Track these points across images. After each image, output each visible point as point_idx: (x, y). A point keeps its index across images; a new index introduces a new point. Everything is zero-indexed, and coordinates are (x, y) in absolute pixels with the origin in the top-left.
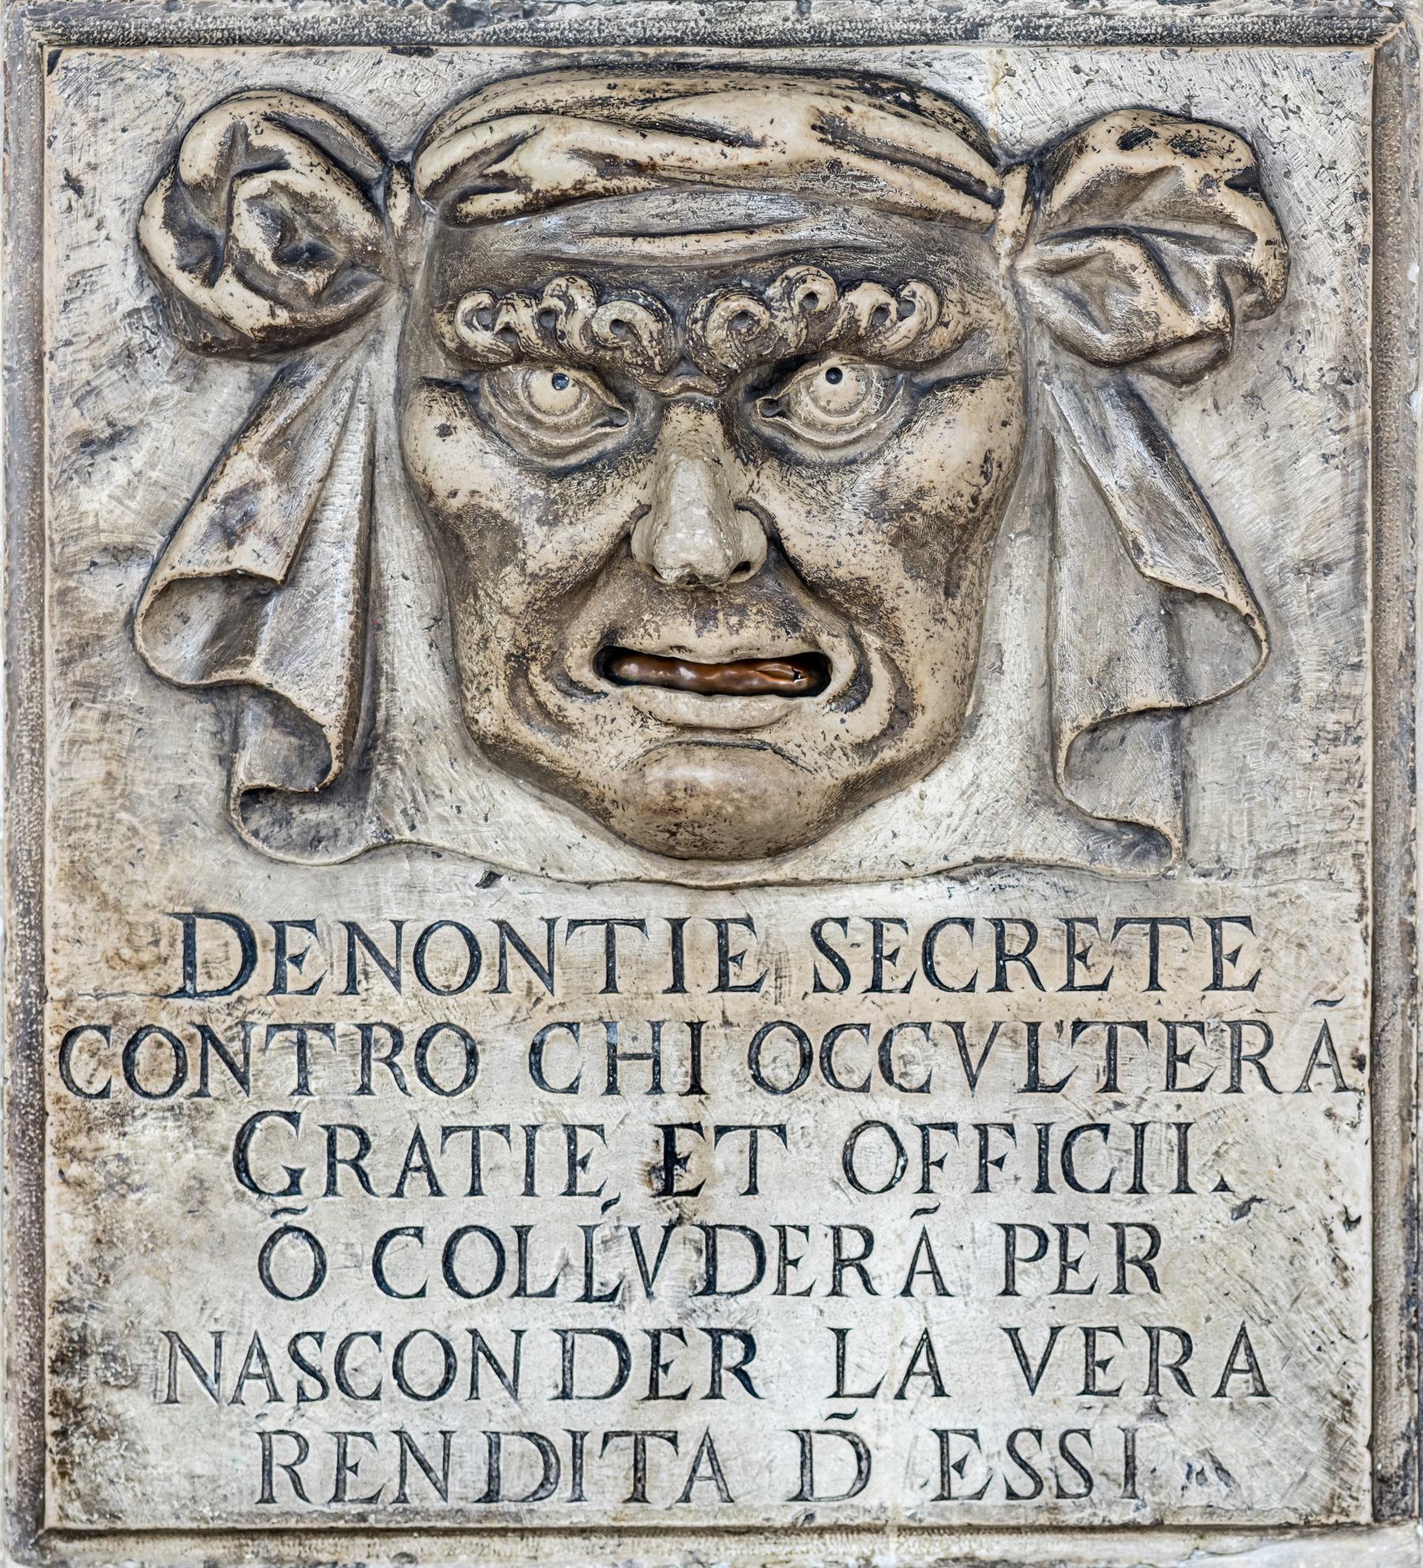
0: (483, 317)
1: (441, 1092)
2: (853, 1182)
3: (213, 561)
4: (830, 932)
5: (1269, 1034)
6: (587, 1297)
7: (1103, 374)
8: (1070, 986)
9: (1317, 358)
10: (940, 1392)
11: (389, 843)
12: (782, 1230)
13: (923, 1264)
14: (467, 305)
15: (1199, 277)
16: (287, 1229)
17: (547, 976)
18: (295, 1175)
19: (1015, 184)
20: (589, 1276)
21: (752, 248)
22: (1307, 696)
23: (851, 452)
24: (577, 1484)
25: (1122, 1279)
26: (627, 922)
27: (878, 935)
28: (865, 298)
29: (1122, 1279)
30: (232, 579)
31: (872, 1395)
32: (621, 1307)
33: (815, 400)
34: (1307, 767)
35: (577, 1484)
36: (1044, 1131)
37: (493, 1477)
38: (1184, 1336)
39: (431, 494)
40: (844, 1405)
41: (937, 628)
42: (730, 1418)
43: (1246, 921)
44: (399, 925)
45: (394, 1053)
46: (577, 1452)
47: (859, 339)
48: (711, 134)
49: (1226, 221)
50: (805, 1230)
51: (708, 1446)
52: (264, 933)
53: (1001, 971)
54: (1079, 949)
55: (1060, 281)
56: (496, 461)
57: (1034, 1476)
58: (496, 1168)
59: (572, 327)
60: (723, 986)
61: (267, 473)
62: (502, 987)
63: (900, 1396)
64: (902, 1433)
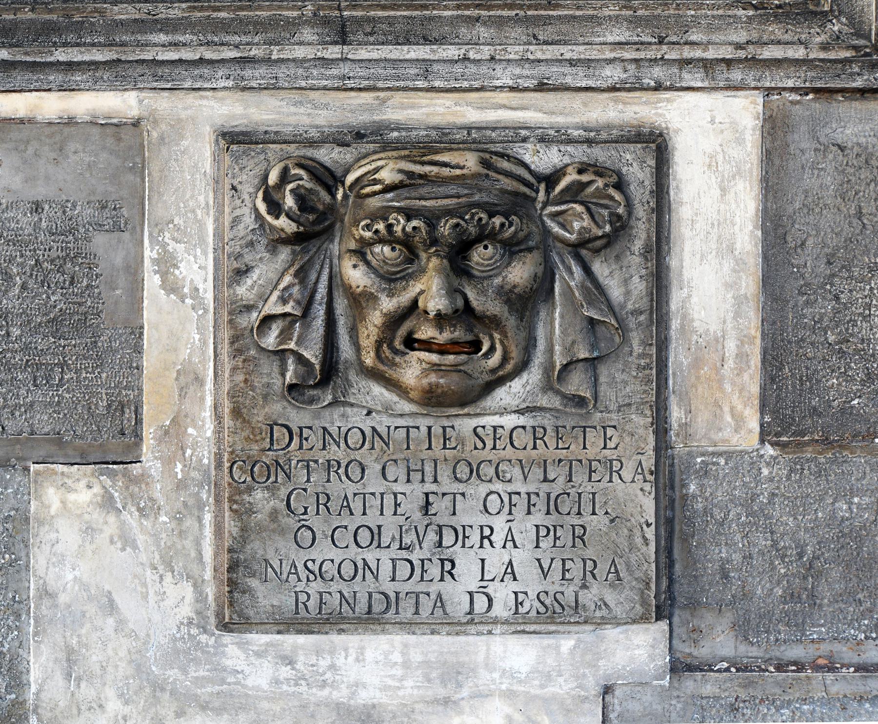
0: (368, 227)
1: (353, 482)
2: (487, 511)
3: (279, 310)
4: (479, 430)
5: (622, 464)
7: (570, 249)
8: (557, 448)
9: (638, 245)
10: (515, 579)
11: (337, 401)
12: (464, 527)
13: (509, 538)
14: (363, 223)
15: (604, 217)
16: (303, 526)
17: (387, 445)
18: (306, 508)
19: (542, 187)
20: (401, 541)
21: (459, 203)
22: (635, 354)
23: (491, 273)
24: (397, 609)
25: (574, 543)
26: (413, 427)
27: (495, 431)
28: (497, 221)
29: (574, 543)
30: (285, 315)
31: (493, 580)
32: (412, 552)
33: (479, 255)
34: (635, 377)
35: (397, 609)
36: (549, 495)
37: (370, 606)
38: (594, 562)
39: (351, 287)
40: (484, 584)
41: (517, 332)
42: (448, 587)
43: (614, 427)
44: (339, 428)
45: (338, 469)
46: (397, 598)
47: (496, 234)
48: (445, 165)
49: (612, 198)
50: (471, 527)
51: (439, 595)
52: (295, 430)
53: (535, 443)
54: (560, 436)
55: (556, 219)
56: (373, 276)
57: (546, 606)
58: (371, 506)
59: (398, 229)
60: (445, 448)
62: (373, 448)
63: (502, 581)
64: (503, 593)
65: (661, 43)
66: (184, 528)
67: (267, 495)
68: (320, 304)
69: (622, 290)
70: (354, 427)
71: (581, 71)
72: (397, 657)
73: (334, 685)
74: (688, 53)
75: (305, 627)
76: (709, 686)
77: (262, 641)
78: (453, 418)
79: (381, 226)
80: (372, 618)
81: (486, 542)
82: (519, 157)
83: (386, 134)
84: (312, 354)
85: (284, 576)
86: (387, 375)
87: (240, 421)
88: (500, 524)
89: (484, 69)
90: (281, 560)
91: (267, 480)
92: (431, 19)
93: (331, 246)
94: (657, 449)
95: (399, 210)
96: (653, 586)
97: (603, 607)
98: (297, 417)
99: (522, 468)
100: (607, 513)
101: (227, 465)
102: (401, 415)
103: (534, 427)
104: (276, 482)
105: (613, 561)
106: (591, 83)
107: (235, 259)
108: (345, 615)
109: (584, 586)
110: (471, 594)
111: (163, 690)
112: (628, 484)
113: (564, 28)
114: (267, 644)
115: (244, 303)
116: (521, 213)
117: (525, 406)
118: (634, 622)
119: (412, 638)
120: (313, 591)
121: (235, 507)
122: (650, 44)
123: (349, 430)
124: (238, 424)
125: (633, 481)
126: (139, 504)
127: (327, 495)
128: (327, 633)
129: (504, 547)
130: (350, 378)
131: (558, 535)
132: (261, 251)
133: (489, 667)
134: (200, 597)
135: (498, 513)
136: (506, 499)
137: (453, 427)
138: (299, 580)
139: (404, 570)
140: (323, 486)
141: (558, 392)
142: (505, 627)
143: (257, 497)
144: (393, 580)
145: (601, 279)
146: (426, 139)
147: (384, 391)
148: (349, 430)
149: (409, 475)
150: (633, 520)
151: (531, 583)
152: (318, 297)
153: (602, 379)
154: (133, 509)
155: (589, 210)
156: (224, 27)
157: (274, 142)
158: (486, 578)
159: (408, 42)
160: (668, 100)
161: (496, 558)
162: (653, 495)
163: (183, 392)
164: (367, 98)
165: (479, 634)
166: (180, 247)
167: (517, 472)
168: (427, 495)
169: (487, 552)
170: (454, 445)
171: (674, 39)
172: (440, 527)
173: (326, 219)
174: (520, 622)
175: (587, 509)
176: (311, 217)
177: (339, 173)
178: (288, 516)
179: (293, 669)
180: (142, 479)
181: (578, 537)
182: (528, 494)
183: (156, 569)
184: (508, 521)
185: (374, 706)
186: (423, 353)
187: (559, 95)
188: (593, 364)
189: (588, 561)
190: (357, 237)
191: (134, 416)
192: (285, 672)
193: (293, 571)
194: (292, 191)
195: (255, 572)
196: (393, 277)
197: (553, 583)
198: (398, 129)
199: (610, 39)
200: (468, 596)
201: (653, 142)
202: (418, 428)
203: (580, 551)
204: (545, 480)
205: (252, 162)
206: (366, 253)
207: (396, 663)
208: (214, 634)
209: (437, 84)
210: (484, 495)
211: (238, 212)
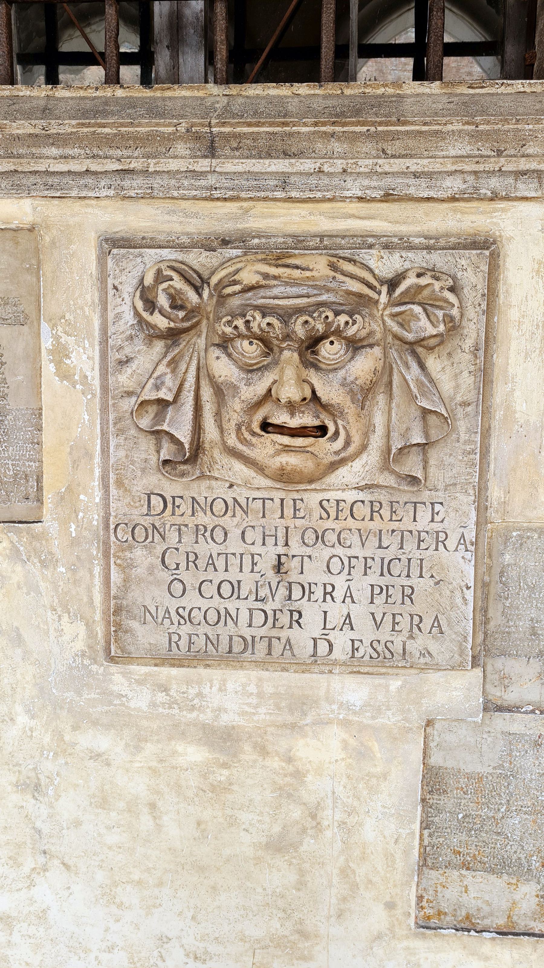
1: (217, 544)
2: (329, 571)
3: (153, 396)
4: (325, 503)
5: (447, 535)
6: (256, 600)
7: (407, 346)
8: (391, 520)
9: (468, 344)
10: (352, 629)
11: (203, 476)
12: (310, 584)
13: (348, 594)
16: (176, 579)
18: (178, 565)
19: (384, 289)
20: (257, 594)
22: (461, 441)
23: (336, 366)
26: (268, 499)
27: (338, 505)
28: (343, 319)
31: (334, 629)
32: (266, 603)
36: (383, 559)
37: (231, 647)
38: (420, 617)
42: (295, 633)
44: (206, 498)
45: (205, 532)
49: (446, 301)
50: (316, 584)
51: (288, 641)
52: (169, 500)
53: (372, 515)
54: (394, 510)
55: (396, 319)
56: (233, 367)
57: (377, 652)
58: (232, 564)
59: (254, 326)
60: (295, 517)
61: (169, 370)
62: (234, 516)
63: (341, 630)
64: (341, 640)
65: (499, 156)
66: (77, 578)
67: (145, 553)
68: (189, 391)
69: (453, 384)
70: (218, 498)
71: (423, 183)
72: (252, 688)
73: (201, 709)
74: (524, 165)
75: (177, 662)
76: (517, 724)
77: (143, 672)
78: (302, 492)
79: (240, 323)
80: (232, 655)
81: (328, 596)
82: (364, 262)
83: (248, 241)
84: (184, 435)
85: (160, 620)
86: (245, 454)
87: (122, 489)
88: (340, 583)
89: (336, 181)
90: (157, 607)
91: (145, 540)
92: (291, 135)
93: (199, 341)
94: (477, 524)
95: (256, 308)
96: (470, 639)
97: (427, 655)
98: (170, 488)
99: (361, 536)
100: (432, 576)
101: (112, 527)
102: (258, 489)
103: (371, 502)
104: (153, 542)
105: (437, 617)
106: (432, 194)
107: (117, 351)
108: (210, 653)
109: (411, 637)
110: (315, 640)
111: (61, 708)
112: (451, 553)
113: (411, 143)
114: (146, 674)
115: (125, 389)
116: (364, 313)
117: (364, 484)
118: (453, 669)
119: (265, 674)
120: (184, 633)
121: (119, 561)
122: (489, 157)
123: (214, 500)
124: (121, 492)
125: (456, 550)
126: (40, 557)
127: (195, 554)
128: (195, 667)
129: (344, 602)
130: (215, 456)
131: (390, 593)
132: (139, 345)
133: (330, 700)
134: (91, 634)
135: (340, 573)
136: (346, 562)
137: (302, 500)
138: (172, 623)
139: (259, 618)
140: (192, 546)
141: (393, 472)
142: (343, 668)
143: (137, 554)
144: (250, 626)
145: (434, 375)
146: (283, 246)
147: (243, 467)
148: (214, 500)
149: (264, 539)
150: (454, 583)
151: (365, 631)
152: (187, 385)
153: (432, 462)
154: (36, 561)
155: (425, 310)
156: (109, 141)
157: (150, 247)
158: (327, 627)
159: (269, 156)
160: (503, 210)
161: (336, 611)
162: (473, 562)
163: (75, 464)
164: (232, 207)
165: (322, 673)
166: (71, 340)
167: (355, 539)
168: (279, 556)
169: (329, 606)
170: (302, 515)
171: (512, 152)
172: (290, 584)
173: (194, 317)
174: (354, 665)
175: (415, 571)
176: (181, 314)
177: (205, 276)
178: (163, 570)
179: (167, 695)
180: (42, 537)
181: (407, 596)
182: (366, 559)
183: (55, 610)
184: (347, 580)
185: (233, 728)
186: (276, 435)
187: (403, 205)
188: (424, 448)
189: (415, 616)
190: (220, 333)
191: (36, 484)
192: (161, 697)
193: (167, 616)
194: (164, 290)
195: (136, 616)
196: (251, 368)
197: (385, 634)
198: (259, 237)
199: (453, 153)
200: (312, 641)
201: (488, 249)
202: (272, 500)
203: (408, 607)
204: (380, 547)
205: (130, 265)
206: (227, 347)
207: (252, 694)
208: (103, 665)
209: (294, 194)
210: (327, 558)
211: (119, 310)
